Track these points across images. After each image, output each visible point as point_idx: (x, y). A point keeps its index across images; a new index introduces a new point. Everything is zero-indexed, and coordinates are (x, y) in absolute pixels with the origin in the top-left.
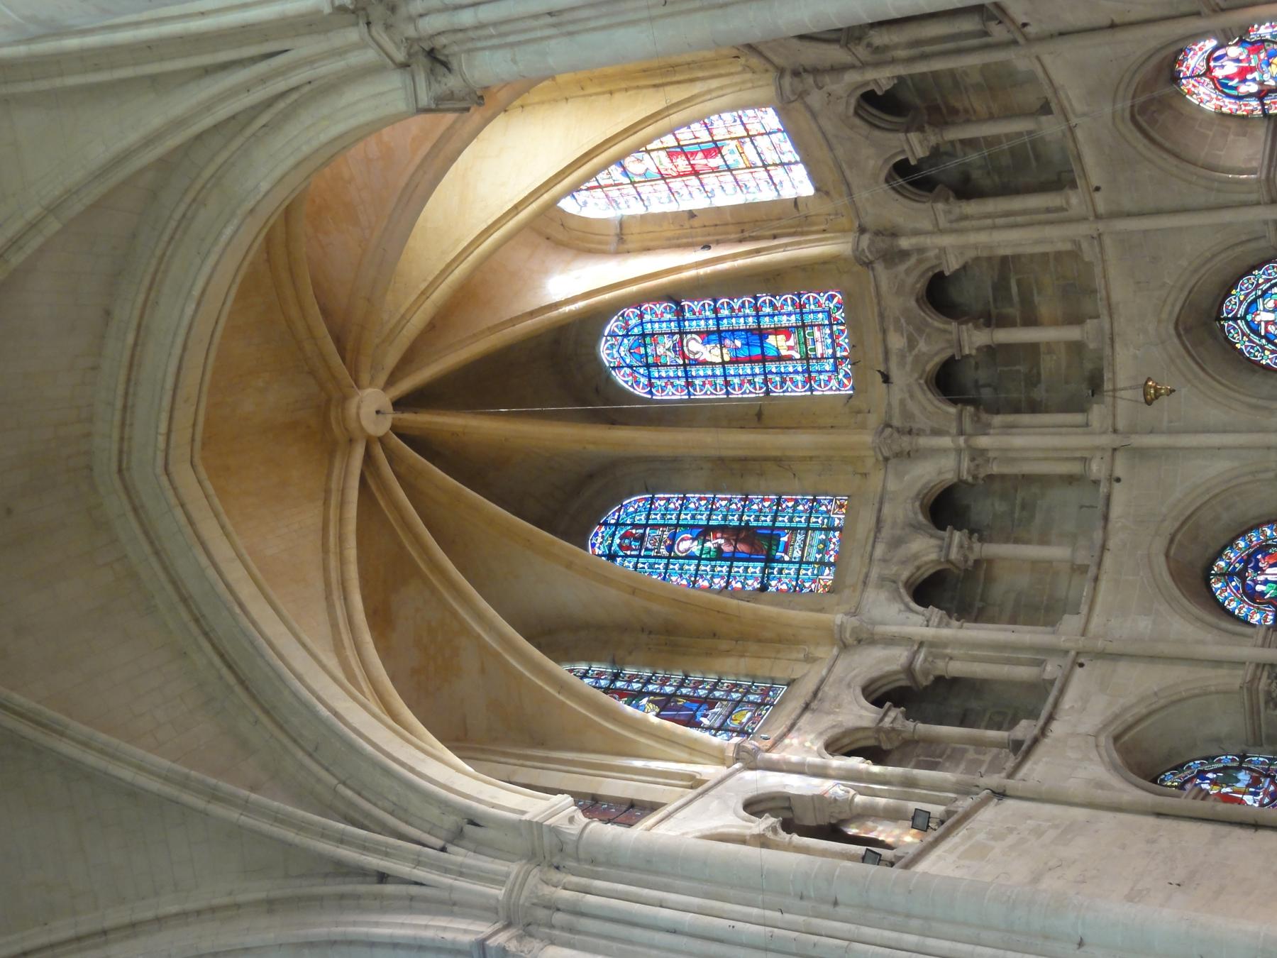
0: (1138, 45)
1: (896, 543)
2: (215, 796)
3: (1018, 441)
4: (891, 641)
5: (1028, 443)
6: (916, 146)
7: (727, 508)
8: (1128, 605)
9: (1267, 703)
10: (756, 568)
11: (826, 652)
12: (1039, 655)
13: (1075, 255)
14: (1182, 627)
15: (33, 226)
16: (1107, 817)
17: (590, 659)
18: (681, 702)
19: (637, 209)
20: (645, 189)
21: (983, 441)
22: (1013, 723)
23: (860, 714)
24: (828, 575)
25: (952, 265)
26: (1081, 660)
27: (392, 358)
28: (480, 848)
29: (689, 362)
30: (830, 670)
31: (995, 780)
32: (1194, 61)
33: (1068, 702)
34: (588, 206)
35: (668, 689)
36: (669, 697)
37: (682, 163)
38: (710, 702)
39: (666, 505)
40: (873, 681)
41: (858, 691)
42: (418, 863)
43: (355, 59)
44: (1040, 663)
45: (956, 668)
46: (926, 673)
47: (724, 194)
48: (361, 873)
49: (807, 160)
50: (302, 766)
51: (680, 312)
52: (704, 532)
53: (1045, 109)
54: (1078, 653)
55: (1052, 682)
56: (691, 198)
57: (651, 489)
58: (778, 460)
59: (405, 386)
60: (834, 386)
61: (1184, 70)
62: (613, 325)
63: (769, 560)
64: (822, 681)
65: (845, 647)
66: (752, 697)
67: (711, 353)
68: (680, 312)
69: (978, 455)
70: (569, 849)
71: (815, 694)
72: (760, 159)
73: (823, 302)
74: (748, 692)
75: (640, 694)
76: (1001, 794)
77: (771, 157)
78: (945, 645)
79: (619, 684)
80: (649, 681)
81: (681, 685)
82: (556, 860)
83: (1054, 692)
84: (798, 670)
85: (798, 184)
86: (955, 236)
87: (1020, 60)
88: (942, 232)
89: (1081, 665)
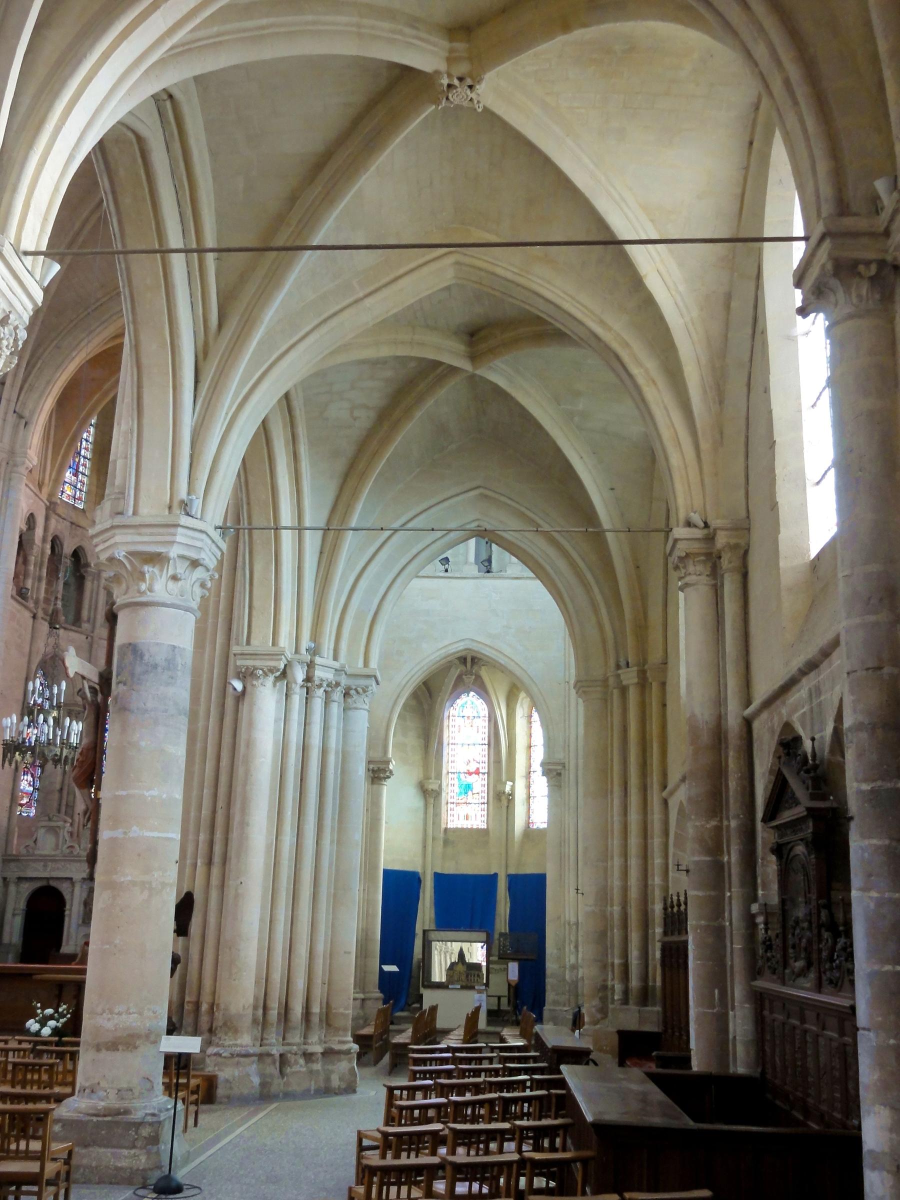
12: (92, 621)
16: (26, 659)
18: (77, 460)
22: (64, 615)
23: (68, 548)
28: (16, 427)
31: (40, 614)
33: (72, 634)
36: (79, 453)
40: (83, 549)
42: (9, 401)
44: (88, 621)
45: (88, 585)
46: (86, 572)
50: (53, 341)
55: (80, 627)
66: (78, 493)
70: (15, 469)
74: (81, 490)
76: (34, 617)
82: (11, 463)
83: (76, 629)
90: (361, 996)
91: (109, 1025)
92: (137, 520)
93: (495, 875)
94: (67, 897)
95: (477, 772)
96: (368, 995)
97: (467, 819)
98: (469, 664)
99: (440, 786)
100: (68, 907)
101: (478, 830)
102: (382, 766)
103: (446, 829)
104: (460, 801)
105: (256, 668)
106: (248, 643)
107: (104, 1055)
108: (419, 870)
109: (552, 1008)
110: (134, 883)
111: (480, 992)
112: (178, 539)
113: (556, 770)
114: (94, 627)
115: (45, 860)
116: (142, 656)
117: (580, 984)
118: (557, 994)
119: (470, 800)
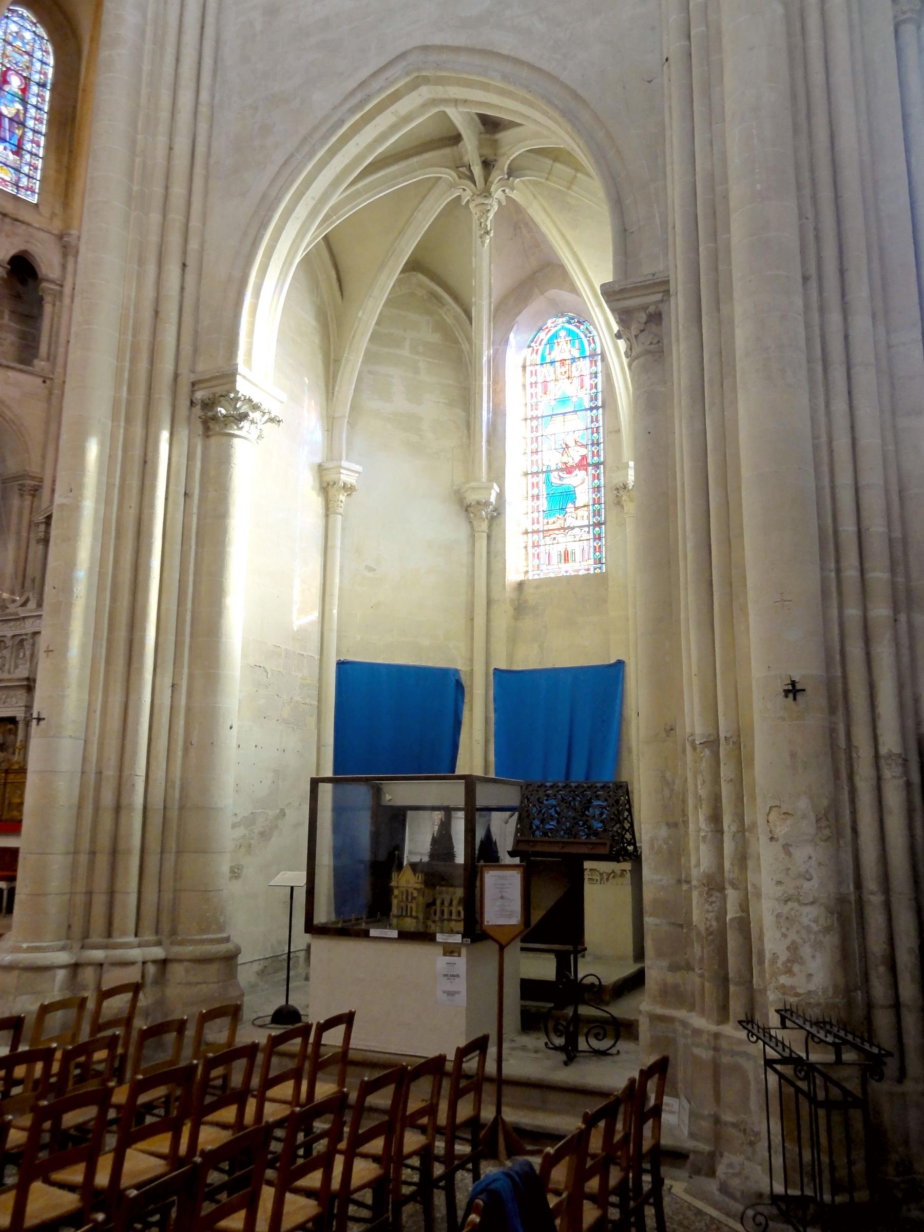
4: (64, 267)
9: (20, 485)
11: (57, 226)
17: (57, 67)
26: (48, 382)
30: (39, 229)
33: (11, 374)
35: (30, 123)
36: (23, 124)
38: (18, 150)
41: (22, 248)
44: (48, 359)
45: (48, 308)
54: (52, 379)
64: (28, 224)
65: (61, 237)
71: (17, 220)
75: (24, 102)
78: (61, 301)
79: (35, 89)
80: (38, 108)
81: (35, 132)
84: (45, 211)
89: (44, 382)
90: (158, 953)
93: (620, 664)
95: (583, 464)
96: (178, 951)
97: (566, 560)
98: (477, 170)
99: (501, 496)
101: (587, 577)
102: (219, 390)
103: (521, 585)
104: (551, 527)
108: (460, 665)
109: (659, 1010)
111: (450, 950)
113: (644, 308)
114: (54, 364)
117: (733, 942)
118: (674, 968)
119: (570, 522)
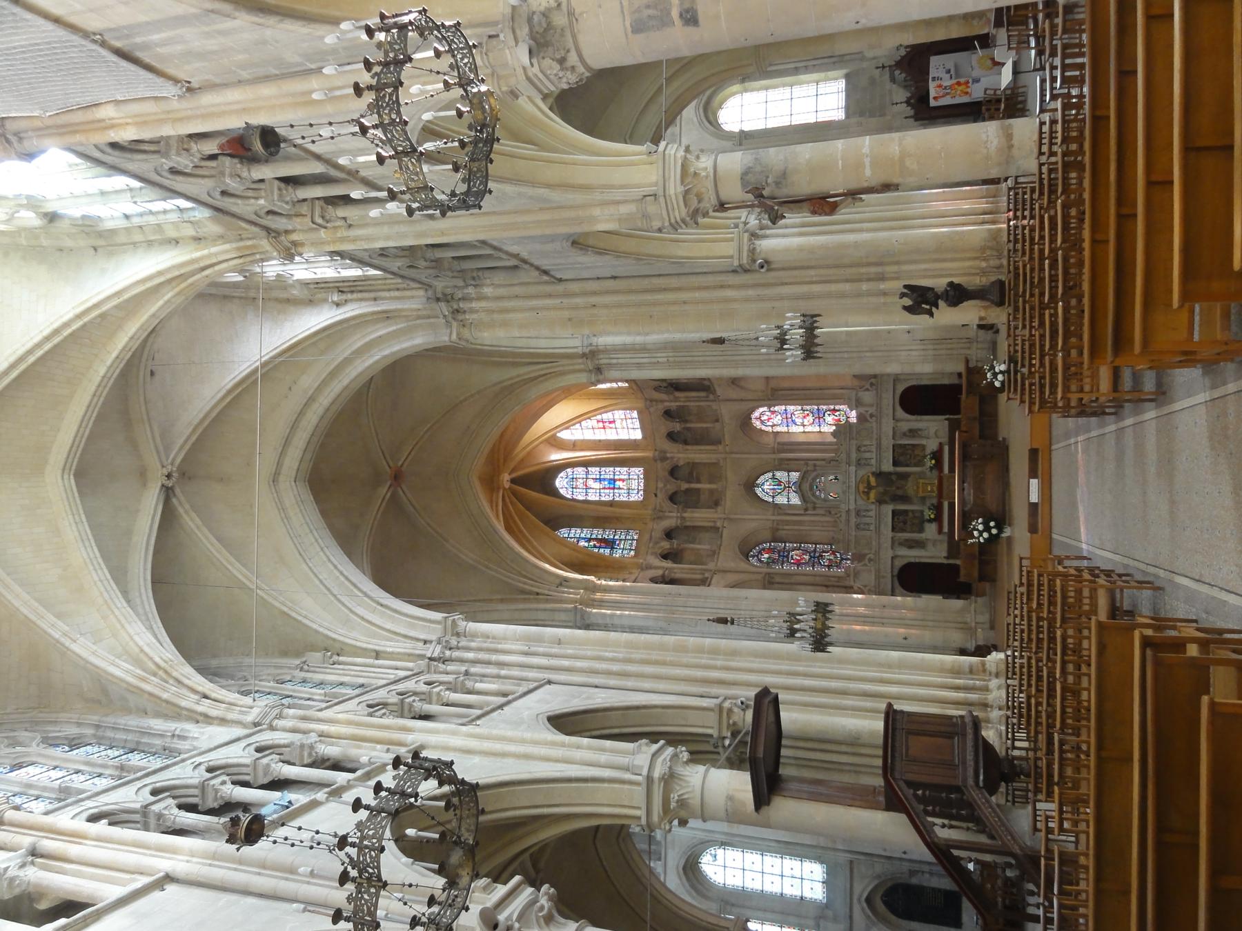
0: (745, 406)
1: (656, 543)
2: (487, 567)
3: (696, 515)
4: (656, 568)
5: (699, 516)
6: (677, 427)
7: (598, 533)
8: (728, 559)
10: (608, 551)
11: (636, 572)
13: (715, 464)
14: (743, 565)
15: (472, 396)
19: (581, 438)
20: (585, 431)
21: (685, 515)
24: (632, 553)
25: (681, 463)
27: (512, 465)
29: (587, 488)
32: (756, 414)
34: (565, 435)
37: (601, 425)
39: (575, 532)
43: (577, 367)
45: (678, 576)
47: (610, 435)
48: (530, 593)
49: (643, 428)
51: (587, 473)
52: (589, 540)
53: (717, 421)
56: (601, 435)
57: (570, 526)
58: (617, 518)
59: (514, 475)
60: (636, 497)
61: (753, 416)
62: (562, 474)
63: (612, 548)
67: (597, 485)
68: (587, 473)
69: (683, 518)
72: (626, 426)
73: (638, 471)
77: (630, 426)
85: (637, 435)
86: (682, 455)
87: (714, 406)
88: (679, 452)
91: (995, 142)
92: (661, 184)
94: (905, 561)
100: (913, 560)
105: (749, 250)
106: (732, 257)
107: (1015, 142)
110: (900, 144)
112: (673, 152)
115: (878, 577)
116: (750, 168)
